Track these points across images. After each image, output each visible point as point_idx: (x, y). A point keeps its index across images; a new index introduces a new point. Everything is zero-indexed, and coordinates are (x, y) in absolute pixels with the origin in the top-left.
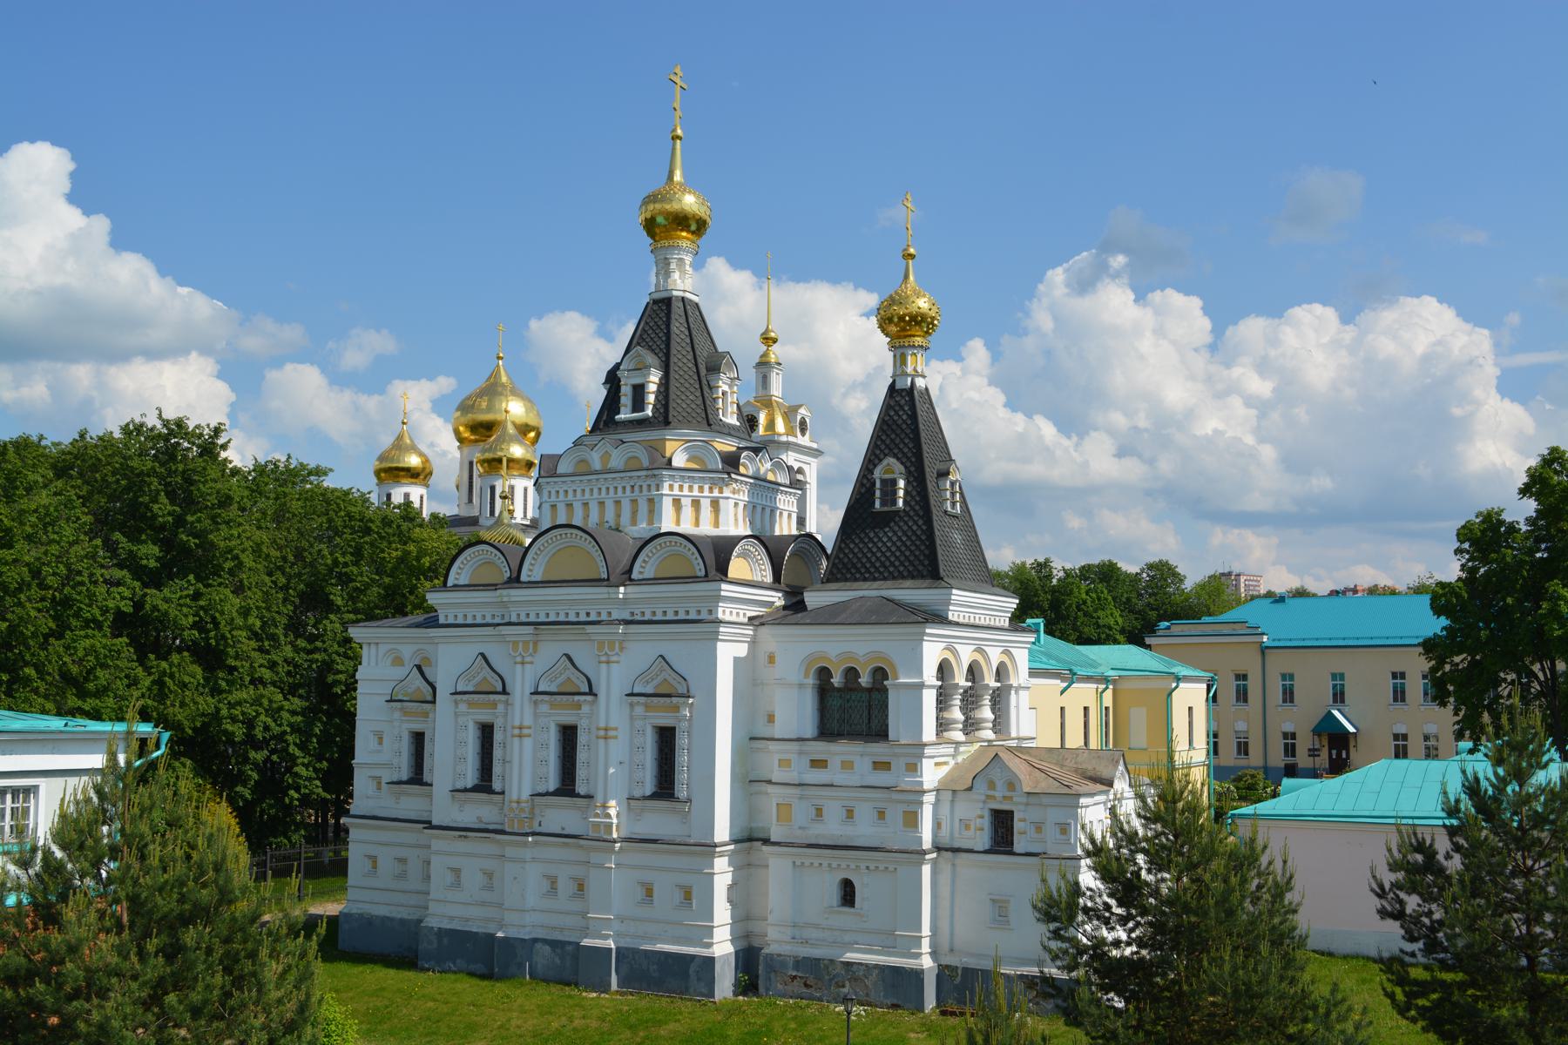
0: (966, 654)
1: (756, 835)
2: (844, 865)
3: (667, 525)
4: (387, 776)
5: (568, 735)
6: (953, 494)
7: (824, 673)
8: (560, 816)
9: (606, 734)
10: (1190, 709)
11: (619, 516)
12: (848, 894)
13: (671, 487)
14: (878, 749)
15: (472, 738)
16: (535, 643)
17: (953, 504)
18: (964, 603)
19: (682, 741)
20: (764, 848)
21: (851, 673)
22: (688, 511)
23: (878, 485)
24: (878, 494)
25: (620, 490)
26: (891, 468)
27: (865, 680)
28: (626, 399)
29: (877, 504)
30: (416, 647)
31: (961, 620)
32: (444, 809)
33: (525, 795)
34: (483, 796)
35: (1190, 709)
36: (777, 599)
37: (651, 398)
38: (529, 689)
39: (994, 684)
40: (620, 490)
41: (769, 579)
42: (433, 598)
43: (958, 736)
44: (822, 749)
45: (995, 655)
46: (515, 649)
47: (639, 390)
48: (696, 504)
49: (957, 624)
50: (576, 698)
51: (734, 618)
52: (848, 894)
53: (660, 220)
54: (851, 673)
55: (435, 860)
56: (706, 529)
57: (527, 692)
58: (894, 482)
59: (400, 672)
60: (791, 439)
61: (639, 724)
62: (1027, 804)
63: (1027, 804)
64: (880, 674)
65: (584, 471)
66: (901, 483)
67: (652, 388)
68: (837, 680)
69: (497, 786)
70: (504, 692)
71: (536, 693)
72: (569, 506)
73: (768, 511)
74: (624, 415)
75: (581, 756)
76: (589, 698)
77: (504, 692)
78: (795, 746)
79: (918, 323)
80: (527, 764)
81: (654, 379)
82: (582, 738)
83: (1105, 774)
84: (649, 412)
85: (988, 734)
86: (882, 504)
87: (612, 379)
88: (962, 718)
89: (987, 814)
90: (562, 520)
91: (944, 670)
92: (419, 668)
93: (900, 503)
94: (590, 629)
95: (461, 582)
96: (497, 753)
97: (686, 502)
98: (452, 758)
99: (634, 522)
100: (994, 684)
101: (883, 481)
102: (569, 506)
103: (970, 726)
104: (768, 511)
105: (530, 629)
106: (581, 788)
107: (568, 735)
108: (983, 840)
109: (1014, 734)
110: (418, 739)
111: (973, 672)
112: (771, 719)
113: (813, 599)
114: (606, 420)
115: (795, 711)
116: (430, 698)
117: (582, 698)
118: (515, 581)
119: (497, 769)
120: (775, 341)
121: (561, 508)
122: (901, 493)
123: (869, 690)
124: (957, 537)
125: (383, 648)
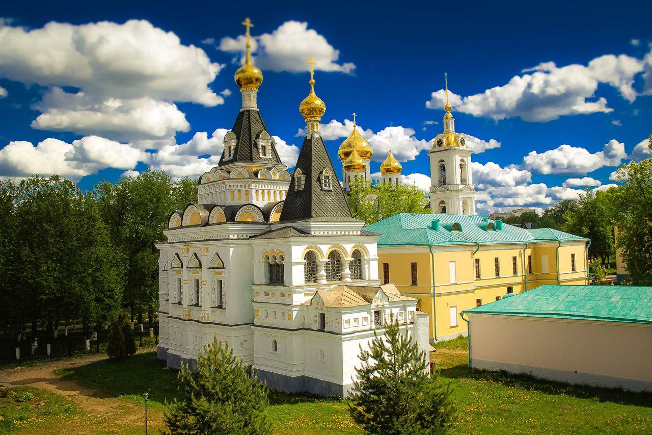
10: (573, 256)
14: (280, 288)
28: (227, 153)
35: (573, 256)
42: (165, 233)
49: (314, 236)
67: (232, 147)
70: (223, 268)
77: (223, 268)
81: (233, 144)
83: (369, 295)
88: (326, 274)
93: (303, 187)
97: (236, 192)
109: (367, 279)
111: (334, 256)
115: (261, 274)
117: (197, 269)
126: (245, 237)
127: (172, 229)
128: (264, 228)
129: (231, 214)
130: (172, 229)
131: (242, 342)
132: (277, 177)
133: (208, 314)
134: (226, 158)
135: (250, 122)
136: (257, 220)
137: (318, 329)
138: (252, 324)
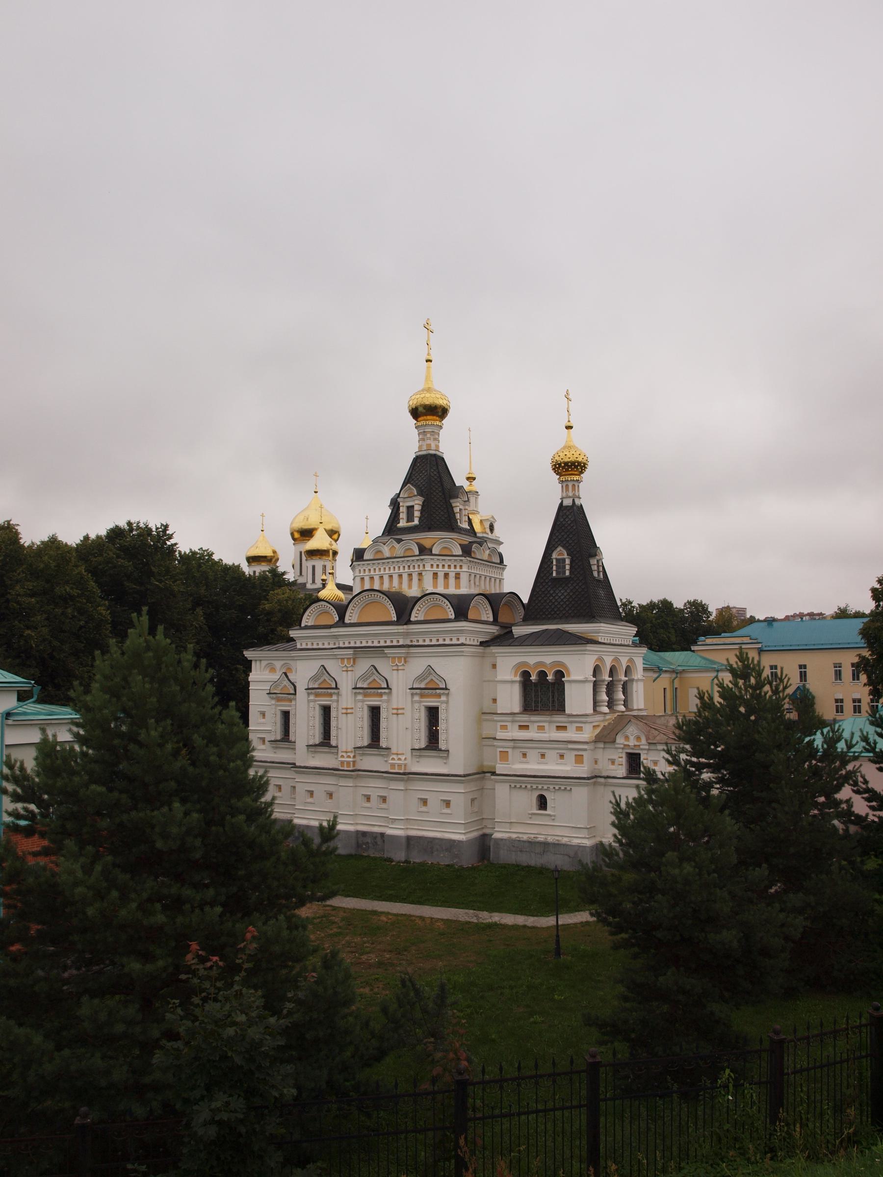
0: (608, 662)
1: (485, 770)
2: (540, 787)
3: (430, 589)
4: (269, 737)
5: (375, 713)
6: (598, 566)
7: (526, 675)
8: (372, 762)
9: (398, 712)
11: (401, 583)
12: (542, 803)
13: (432, 565)
14: (559, 719)
15: (317, 714)
16: (354, 660)
17: (599, 572)
18: (604, 630)
19: (442, 715)
20: (493, 777)
21: (542, 674)
22: (452, 580)
23: (554, 563)
24: (554, 568)
25: (401, 568)
26: (561, 553)
27: (550, 678)
28: (403, 515)
29: (554, 574)
30: (283, 662)
31: (606, 641)
32: (302, 757)
33: (350, 748)
34: (326, 749)
36: (494, 630)
37: (417, 514)
38: (351, 686)
39: (624, 678)
40: (401, 568)
41: (491, 619)
42: (293, 633)
43: (606, 709)
44: (525, 718)
45: (624, 662)
46: (342, 663)
47: (410, 509)
48: (446, 575)
49: (604, 644)
50: (380, 691)
51: (471, 643)
52: (542, 803)
53: (421, 409)
54: (542, 674)
55: (298, 786)
56: (452, 590)
57: (350, 688)
58: (564, 560)
59: (275, 677)
60: (485, 535)
61: (416, 706)
62: (649, 750)
63: (649, 750)
64: (560, 674)
65: (379, 559)
66: (568, 561)
67: (417, 508)
68: (533, 678)
69: (333, 742)
71: (355, 688)
72: (372, 578)
73: (498, 581)
74: (402, 524)
75: (383, 724)
76: (387, 691)
78: (509, 718)
79: (576, 467)
80: (350, 730)
81: (417, 503)
82: (383, 714)
84: (416, 522)
85: (622, 708)
86: (557, 574)
87: (395, 504)
89: (624, 755)
90: (367, 587)
91: (596, 671)
92: (285, 674)
93: (567, 573)
94: (387, 651)
95: (309, 624)
96: (333, 723)
98: (305, 728)
99: (410, 587)
100: (624, 678)
101: (557, 559)
102: (372, 578)
103: (611, 704)
104: (498, 581)
105: (351, 651)
106: (383, 743)
107: (375, 713)
108: (622, 771)
110: (286, 715)
111: (612, 672)
112: (495, 701)
113: (519, 631)
114: (391, 529)
115: (510, 698)
116: (293, 692)
118: (341, 623)
119: (333, 732)
120: (474, 479)
121: (367, 579)
122: (568, 567)
123: (553, 684)
124: (602, 593)
125: (264, 663)
126: (476, 643)
127: (307, 627)
128: (494, 630)
129: (461, 607)
130: (307, 627)
131: (473, 800)
132: (486, 557)
133: (405, 759)
134: (402, 524)
135: (438, 472)
136: (484, 618)
137: (625, 775)
138: (494, 773)
